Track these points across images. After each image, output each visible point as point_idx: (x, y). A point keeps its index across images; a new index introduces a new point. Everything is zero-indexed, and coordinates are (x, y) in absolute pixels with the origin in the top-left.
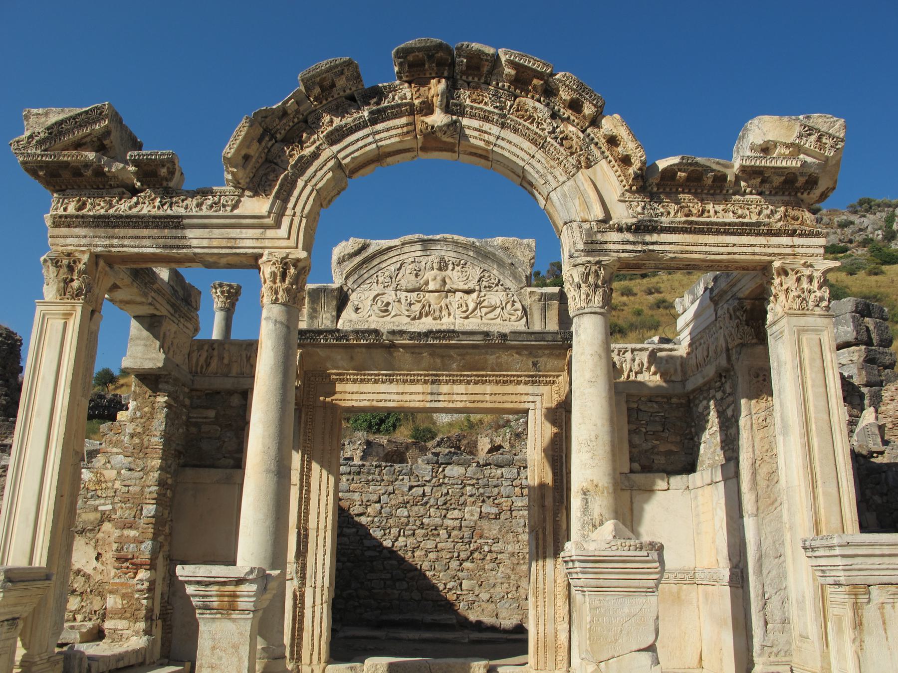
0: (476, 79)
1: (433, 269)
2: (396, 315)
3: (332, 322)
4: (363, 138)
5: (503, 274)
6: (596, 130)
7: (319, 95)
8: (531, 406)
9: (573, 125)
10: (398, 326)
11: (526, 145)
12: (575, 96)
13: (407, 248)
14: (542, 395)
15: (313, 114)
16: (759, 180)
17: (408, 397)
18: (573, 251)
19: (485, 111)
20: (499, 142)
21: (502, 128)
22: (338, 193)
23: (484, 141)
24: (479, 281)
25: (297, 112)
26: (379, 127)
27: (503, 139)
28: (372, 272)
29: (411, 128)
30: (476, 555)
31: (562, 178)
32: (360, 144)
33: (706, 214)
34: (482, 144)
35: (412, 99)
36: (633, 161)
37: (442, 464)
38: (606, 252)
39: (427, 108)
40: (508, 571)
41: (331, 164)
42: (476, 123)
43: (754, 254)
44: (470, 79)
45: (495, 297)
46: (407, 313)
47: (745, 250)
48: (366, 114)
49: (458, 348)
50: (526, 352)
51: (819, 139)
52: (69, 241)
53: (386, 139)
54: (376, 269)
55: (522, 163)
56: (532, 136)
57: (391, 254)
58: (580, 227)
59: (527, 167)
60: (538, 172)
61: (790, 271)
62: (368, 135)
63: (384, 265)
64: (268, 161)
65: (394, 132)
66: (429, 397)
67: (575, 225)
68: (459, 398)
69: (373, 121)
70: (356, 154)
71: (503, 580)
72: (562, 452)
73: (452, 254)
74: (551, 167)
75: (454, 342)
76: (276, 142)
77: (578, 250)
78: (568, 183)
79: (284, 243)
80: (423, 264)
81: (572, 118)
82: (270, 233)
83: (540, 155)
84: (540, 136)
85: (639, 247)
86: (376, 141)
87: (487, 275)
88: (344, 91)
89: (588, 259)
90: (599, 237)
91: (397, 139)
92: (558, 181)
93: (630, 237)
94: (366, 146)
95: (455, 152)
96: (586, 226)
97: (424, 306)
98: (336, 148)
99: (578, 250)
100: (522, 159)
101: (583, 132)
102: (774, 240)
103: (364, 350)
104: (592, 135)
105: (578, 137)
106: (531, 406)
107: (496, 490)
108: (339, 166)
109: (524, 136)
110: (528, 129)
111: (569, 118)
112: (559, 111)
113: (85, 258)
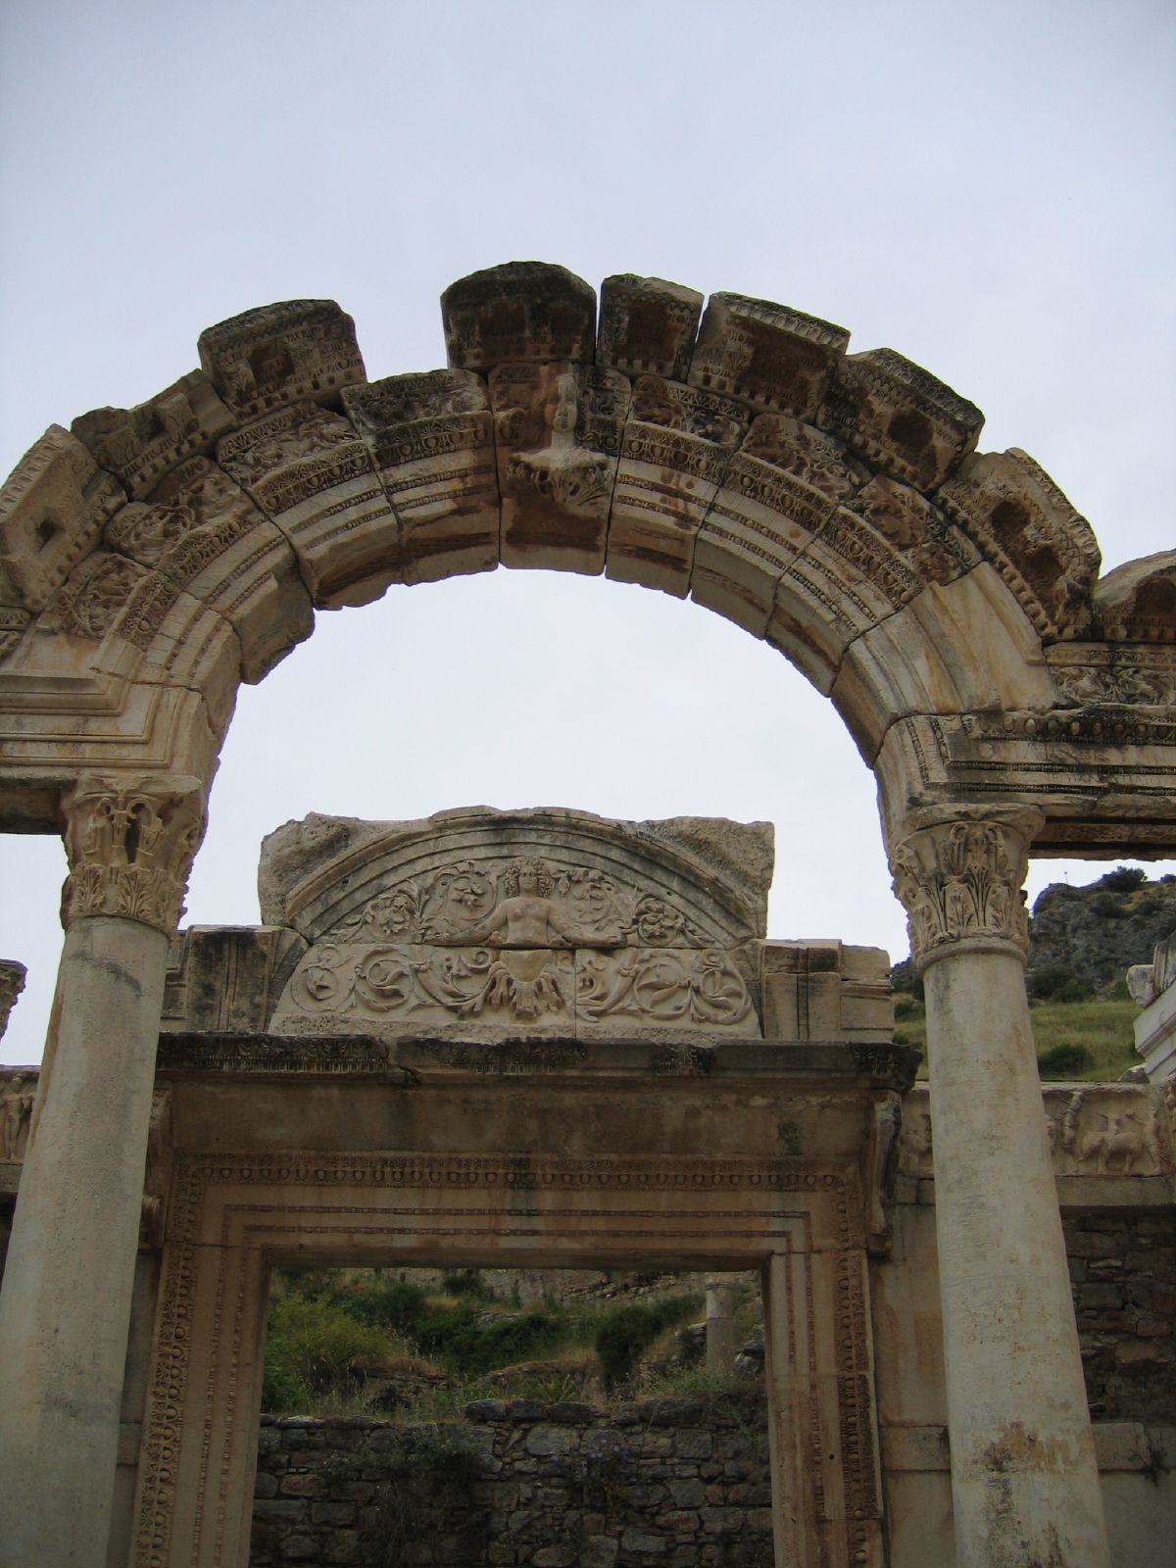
0: (653, 368)
1: (515, 891)
2: (421, 1006)
3: (254, 1020)
4: (362, 499)
5: (695, 905)
6: (961, 492)
7: (249, 387)
8: (778, 1245)
9: (902, 482)
10: (426, 1033)
11: (783, 526)
12: (907, 407)
13: (452, 840)
14: (806, 1215)
15: (232, 437)
17: (447, 1223)
18: (918, 787)
19: (677, 442)
20: (714, 519)
21: (721, 485)
22: (288, 649)
23: (675, 514)
24: (635, 922)
25: (191, 428)
26: (402, 473)
27: (725, 512)
28: (360, 896)
29: (484, 479)
31: (881, 608)
32: (353, 513)
34: (669, 522)
35: (489, 407)
36: (1063, 560)
37: (517, 1422)
38: (1008, 790)
39: (533, 430)
42: (652, 473)
45: (679, 964)
46: (449, 1001)
48: (369, 441)
49: (584, 1088)
50: (759, 1101)
53: (421, 502)
54: (372, 888)
55: (773, 571)
56: (799, 503)
57: (411, 853)
58: (935, 727)
59: (787, 580)
62: (370, 495)
64: (104, 542)
65: (441, 487)
66: (510, 1223)
67: (920, 722)
68: (585, 1225)
69: (387, 456)
70: (343, 538)
72: (865, 1366)
73: (565, 855)
74: (851, 579)
75: (574, 1073)
76: (131, 500)
77: (929, 786)
78: (899, 619)
80: (493, 878)
82: (97, 727)
83: (818, 550)
84: (820, 502)
85: (1094, 781)
86: (395, 508)
87: (655, 906)
88: (316, 385)
89: (962, 807)
90: (987, 752)
91: (448, 505)
92: (870, 615)
93: (1067, 752)
94: (367, 518)
95: (595, 549)
96: (951, 725)
97: (493, 985)
98: (287, 520)
99: (929, 786)
100: (779, 563)
101: (930, 495)
103: (335, 1092)
104: (952, 503)
105: (916, 510)
106: (778, 1245)
107: (659, 1492)
109: (782, 506)
110: (790, 485)
111: (891, 461)
112: (865, 445)
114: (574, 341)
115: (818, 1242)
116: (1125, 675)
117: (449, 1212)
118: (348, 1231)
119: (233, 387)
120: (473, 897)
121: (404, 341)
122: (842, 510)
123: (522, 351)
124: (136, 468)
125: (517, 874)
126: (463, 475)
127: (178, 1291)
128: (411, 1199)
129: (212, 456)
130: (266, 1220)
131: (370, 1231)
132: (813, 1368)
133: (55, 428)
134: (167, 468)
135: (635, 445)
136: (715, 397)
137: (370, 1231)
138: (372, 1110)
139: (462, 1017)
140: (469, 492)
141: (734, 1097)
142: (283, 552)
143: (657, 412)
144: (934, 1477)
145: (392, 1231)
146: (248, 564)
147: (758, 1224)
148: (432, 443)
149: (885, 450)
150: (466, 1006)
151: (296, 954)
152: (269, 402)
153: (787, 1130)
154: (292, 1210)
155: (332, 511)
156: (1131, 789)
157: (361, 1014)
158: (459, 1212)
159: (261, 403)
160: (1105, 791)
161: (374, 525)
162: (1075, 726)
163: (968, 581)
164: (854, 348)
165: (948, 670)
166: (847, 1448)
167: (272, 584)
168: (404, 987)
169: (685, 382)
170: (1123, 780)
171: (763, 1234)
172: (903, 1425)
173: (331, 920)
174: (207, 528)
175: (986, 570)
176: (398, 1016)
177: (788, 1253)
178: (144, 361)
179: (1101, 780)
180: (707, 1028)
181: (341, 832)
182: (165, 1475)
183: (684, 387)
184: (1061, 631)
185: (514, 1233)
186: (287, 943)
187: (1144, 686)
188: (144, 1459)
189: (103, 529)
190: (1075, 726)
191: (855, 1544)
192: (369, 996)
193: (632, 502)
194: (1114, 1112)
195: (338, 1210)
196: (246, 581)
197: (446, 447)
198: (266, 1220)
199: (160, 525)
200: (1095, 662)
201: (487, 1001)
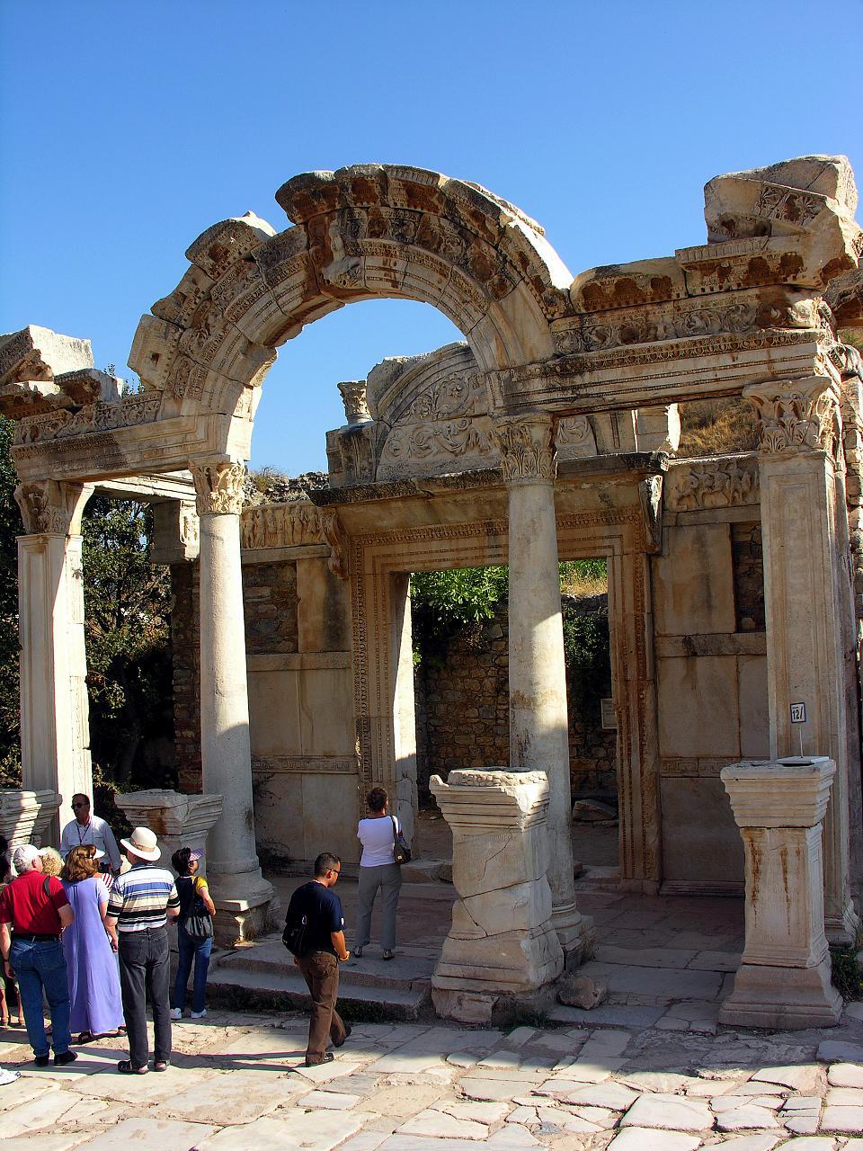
0: (372, 204)
3: (371, 470)
8: (608, 552)
15: (214, 289)
16: (715, 275)
17: (462, 555)
19: (385, 246)
20: (409, 280)
25: (197, 292)
26: (279, 289)
32: (265, 314)
33: (652, 332)
35: (308, 248)
41: (240, 345)
43: (717, 380)
44: (365, 204)
47: (704, 376)
50: (585, 486)
51: (790, 203)
57: (428, 373)
58: (499, 378)
60: (451, 311)
61: (765, 400)
62: (270, 303)
63: (421, 389)
64: (182, 353)
66: (488, 552)
69: (273, 283)
70: (263, 328)
75: (496, 484)
76: (184, 329)
78: (484, 321)
79: (204, 447)
81: (481, 233)
85: (569, 394)
88: (240, 253)
92: (473, 321)
93: (556, 381)
96: (505, 375)
98: (241, 324)
101: (496, 248)
102: (743, 357)
103: (400, 504)
104: (504, 252)
106: (608, 552)
114: (335, 201)
115: (626, 550)
116: (587, 334)
117: (462, 550)
118: (421, 562)
119: (206, 269)
120: (457, 393)
121: (267, 222)
123: (316, 211)
124: (181, 317)
126: (303, 284)
127: (357, 595)
128: (446, 545)
129: (210, 299)
130: (389, 560)
131: (430, 561)
132: (624, 610)
133: (145, 316)
134: (194, 311)
135: (369, 250)
136: (401, 212)
137: (430, 561)
138: (417, 508)
139: (456, 456)
140: (306, 292)
141: (573, 485)
142: (242, 339)
144: (679, 660)
145: (440, 560)
146: (230, 349)
147: (599, 543)
148: (287, 272)
149: (473, 226)
151: (386, 434)
152: (224, 268)
153: (603, 497)
154: (399, 555)
155: (258, 315)
156: (587, 396)
157: (413, 459)
158: (467, 549)
159: (220, 270)
160: (575, 398)
161: (273, 318)
162: (558, 369)
163: (516, 292)
164: (442, 183)
165: (503, 346)
166: (638, 649)
167: (241, 357)
168: (431, 443)
169: (388, 206)
170: (583, 392)
171: (601, 547)
172: (666, 636)
173: (399, 413)
174: (211, 339)
175: (522, 285)
176: (429, 458)
178: (167, 273)
179: (573, 393)
181: (397, 370)
182: (363, 671)
183: (388, 209)
184: (553, 315)
185: (490, 556)
186: (380, 431)
187: (596, 339)
188: (353, 666)
189: (176, 347)
190: (558, 369)
191: (640, 691)
195: (417, 553)
196: (231, 358)
197: (294, 272)
198: (389, 560)
199: (196, 341)
200: (573, 327)
201: (467, 445)
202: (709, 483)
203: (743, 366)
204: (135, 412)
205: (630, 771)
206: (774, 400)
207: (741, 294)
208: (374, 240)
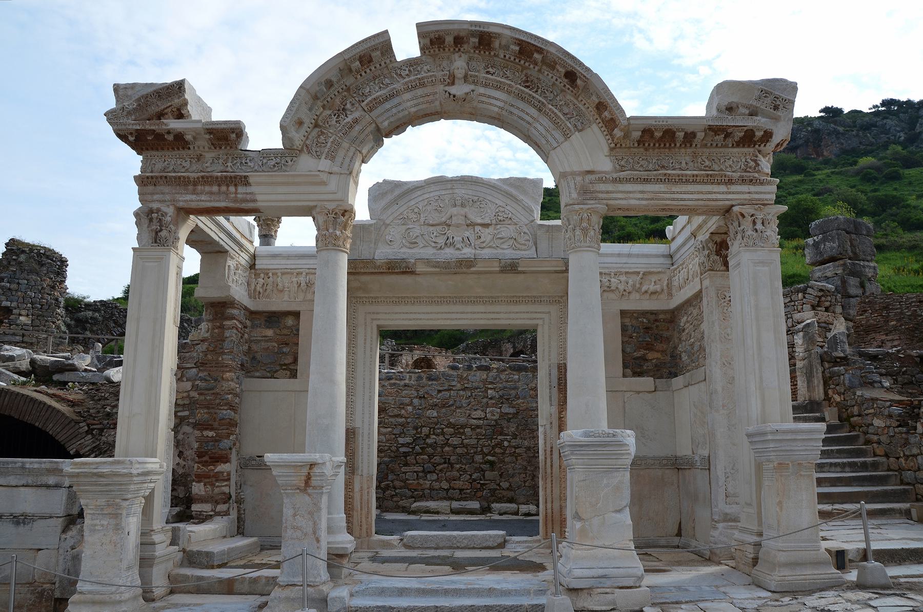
2: (425, 246)
30: (497, 450)
40: (525, 463)
52: (156, 197)
57: (419, 193)
61: (746, 215)
63: (413, 203)
64: (316, 126)
70: (392, 119)
71: (521, 471)
73: (470, 192)
102: (734, 188)
106: (540, 322)
108: (378, 129)
110: (533, 97)
113: (170, 211)
122: (550, 106)
125: (455, 200)
142: (374, 125)
143: (490, 70)
150: (439, 246)
155: (388, 110)
159: (363, 74)
166: (559, 384)
174: (349, 119)
177: (543, 325)
180: (518, 252)
189: (316, 121)
192: (408, 245)
193: (482, 102)
194: (654, 278)
201: (446, 244)
202: (607, 284)
203: (733, 193)
204: (273, 163)
205: (552, 466)
206: (752, 216)
207: (735, 150)
208: (489, 76)
